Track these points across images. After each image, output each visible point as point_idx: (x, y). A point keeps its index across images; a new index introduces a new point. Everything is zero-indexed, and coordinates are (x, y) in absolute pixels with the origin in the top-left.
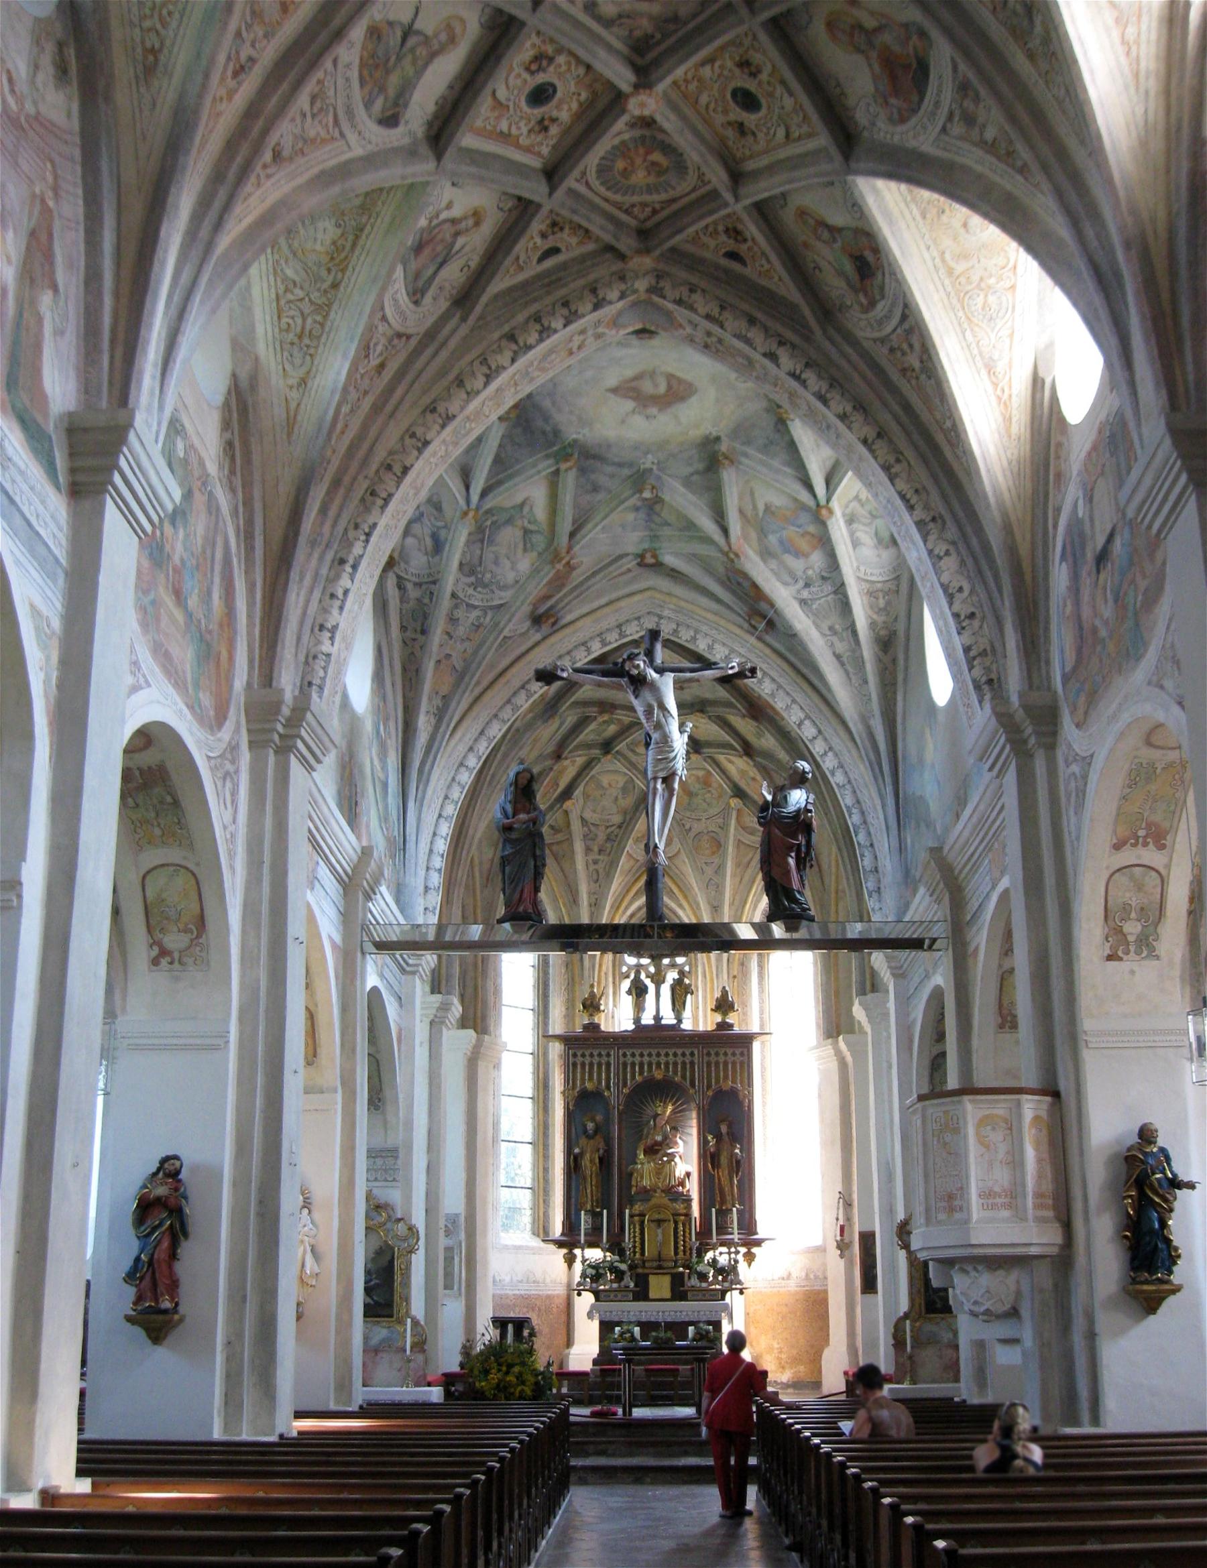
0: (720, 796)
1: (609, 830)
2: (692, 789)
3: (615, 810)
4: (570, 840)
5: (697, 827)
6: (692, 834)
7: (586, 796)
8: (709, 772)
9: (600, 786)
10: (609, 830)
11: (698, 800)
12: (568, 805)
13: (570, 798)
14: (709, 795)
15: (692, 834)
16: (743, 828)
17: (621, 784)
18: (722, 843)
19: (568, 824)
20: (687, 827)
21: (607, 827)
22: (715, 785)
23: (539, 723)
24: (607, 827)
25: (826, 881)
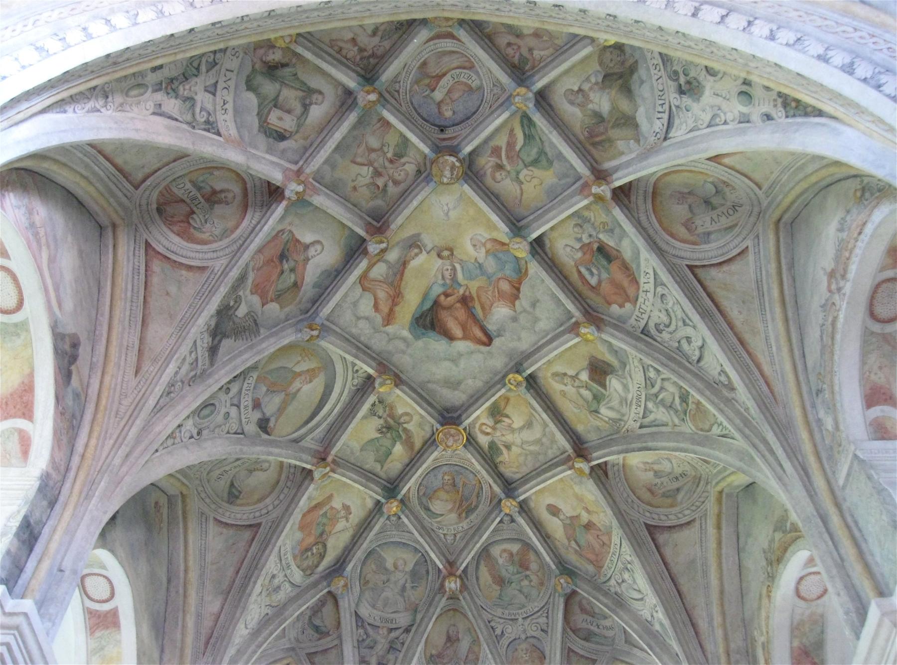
0: (542, 584)
1: (393, 635)
2: (504, 573)
3: (401, 606)
4: (339, 647)
5: (512, 631)
6: (505, 642)
7: (365, 582)
8: (527, 546)
9: (382, 568)
10: (393, 635)
11: (511, 591)
12: (338, 585)
13: (341, 575)
14: (525, 583)
15: (505, 642)
16: (574, 631)
17: (410, 567)
18: (547, 653)
19: (338, 625)
20: (498, 632)
21: (391, 630)
22: (534, 566)
23: (289, 331)
24: (391, 630)
25: (709, 647)
